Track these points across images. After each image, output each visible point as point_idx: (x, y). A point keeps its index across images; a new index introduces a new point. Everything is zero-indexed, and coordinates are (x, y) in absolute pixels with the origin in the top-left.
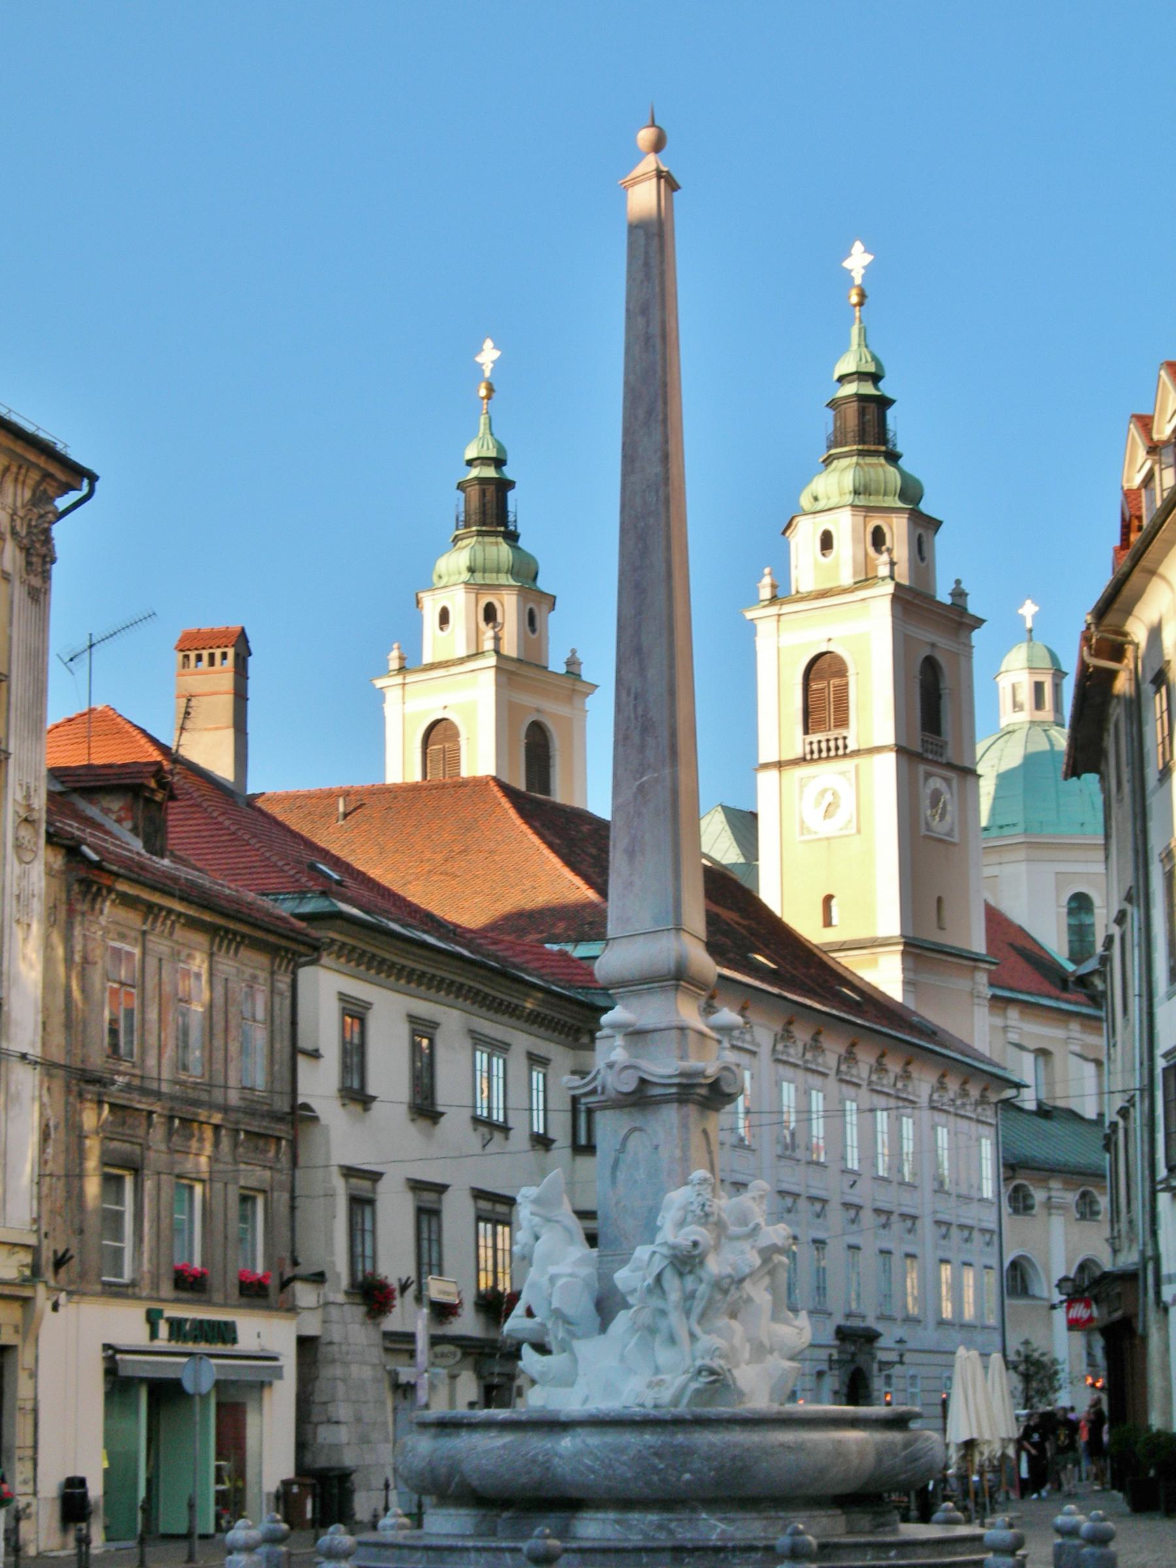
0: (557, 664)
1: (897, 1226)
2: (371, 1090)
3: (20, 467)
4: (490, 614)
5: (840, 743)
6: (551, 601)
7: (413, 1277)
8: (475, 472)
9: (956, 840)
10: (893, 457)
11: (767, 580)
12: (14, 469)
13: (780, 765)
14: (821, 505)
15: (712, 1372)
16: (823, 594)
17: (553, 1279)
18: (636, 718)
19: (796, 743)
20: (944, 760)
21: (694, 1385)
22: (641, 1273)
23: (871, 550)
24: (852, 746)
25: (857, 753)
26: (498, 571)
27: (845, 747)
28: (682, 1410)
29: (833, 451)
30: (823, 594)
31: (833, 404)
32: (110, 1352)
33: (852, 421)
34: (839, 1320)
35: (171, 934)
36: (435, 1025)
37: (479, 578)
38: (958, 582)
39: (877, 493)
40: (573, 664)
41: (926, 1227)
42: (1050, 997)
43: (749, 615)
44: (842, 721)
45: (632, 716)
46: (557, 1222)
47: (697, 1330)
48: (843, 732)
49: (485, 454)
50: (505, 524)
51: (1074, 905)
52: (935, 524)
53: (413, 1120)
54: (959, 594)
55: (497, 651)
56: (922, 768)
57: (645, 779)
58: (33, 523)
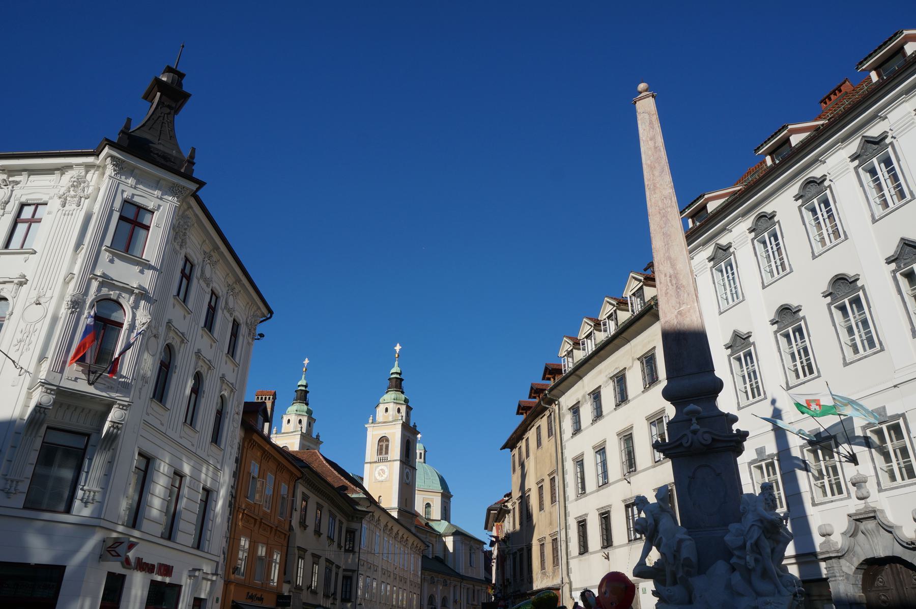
0: (314, 436)
2: (307, 524)
3: (252, 304)
4: (300, 422)
5: (386, 458)
6: (315, 420)
8: (300, 388)
10: (403, 393)
11: (371, 418)
12: (250, 304)
13: (370, 463)
14: (385, 402)
16: (384, 422)
18: (672, 285)
19: (375, 458)
22: (742, 537)
23: (397, 413)
26: (303, 412)
30: (384, 422)
31: (390, 379)
32: (235, 603)
33: (394, 384)
35: (268, 462)
36: (322, 507)
37: (298, 413)
38: (415, 423)
39: (399, 400)
40: (318, 436)
43: (366, 426)
44: (387, 453)
45: (669, 284)
46: (668, 512)
48: (386, 456)
49: (303, 384)
50: (306, 401)
52: (411, 409)
53: (315, 535)
54: (415, 426)
55: (301, 430)
57: (681, 309)
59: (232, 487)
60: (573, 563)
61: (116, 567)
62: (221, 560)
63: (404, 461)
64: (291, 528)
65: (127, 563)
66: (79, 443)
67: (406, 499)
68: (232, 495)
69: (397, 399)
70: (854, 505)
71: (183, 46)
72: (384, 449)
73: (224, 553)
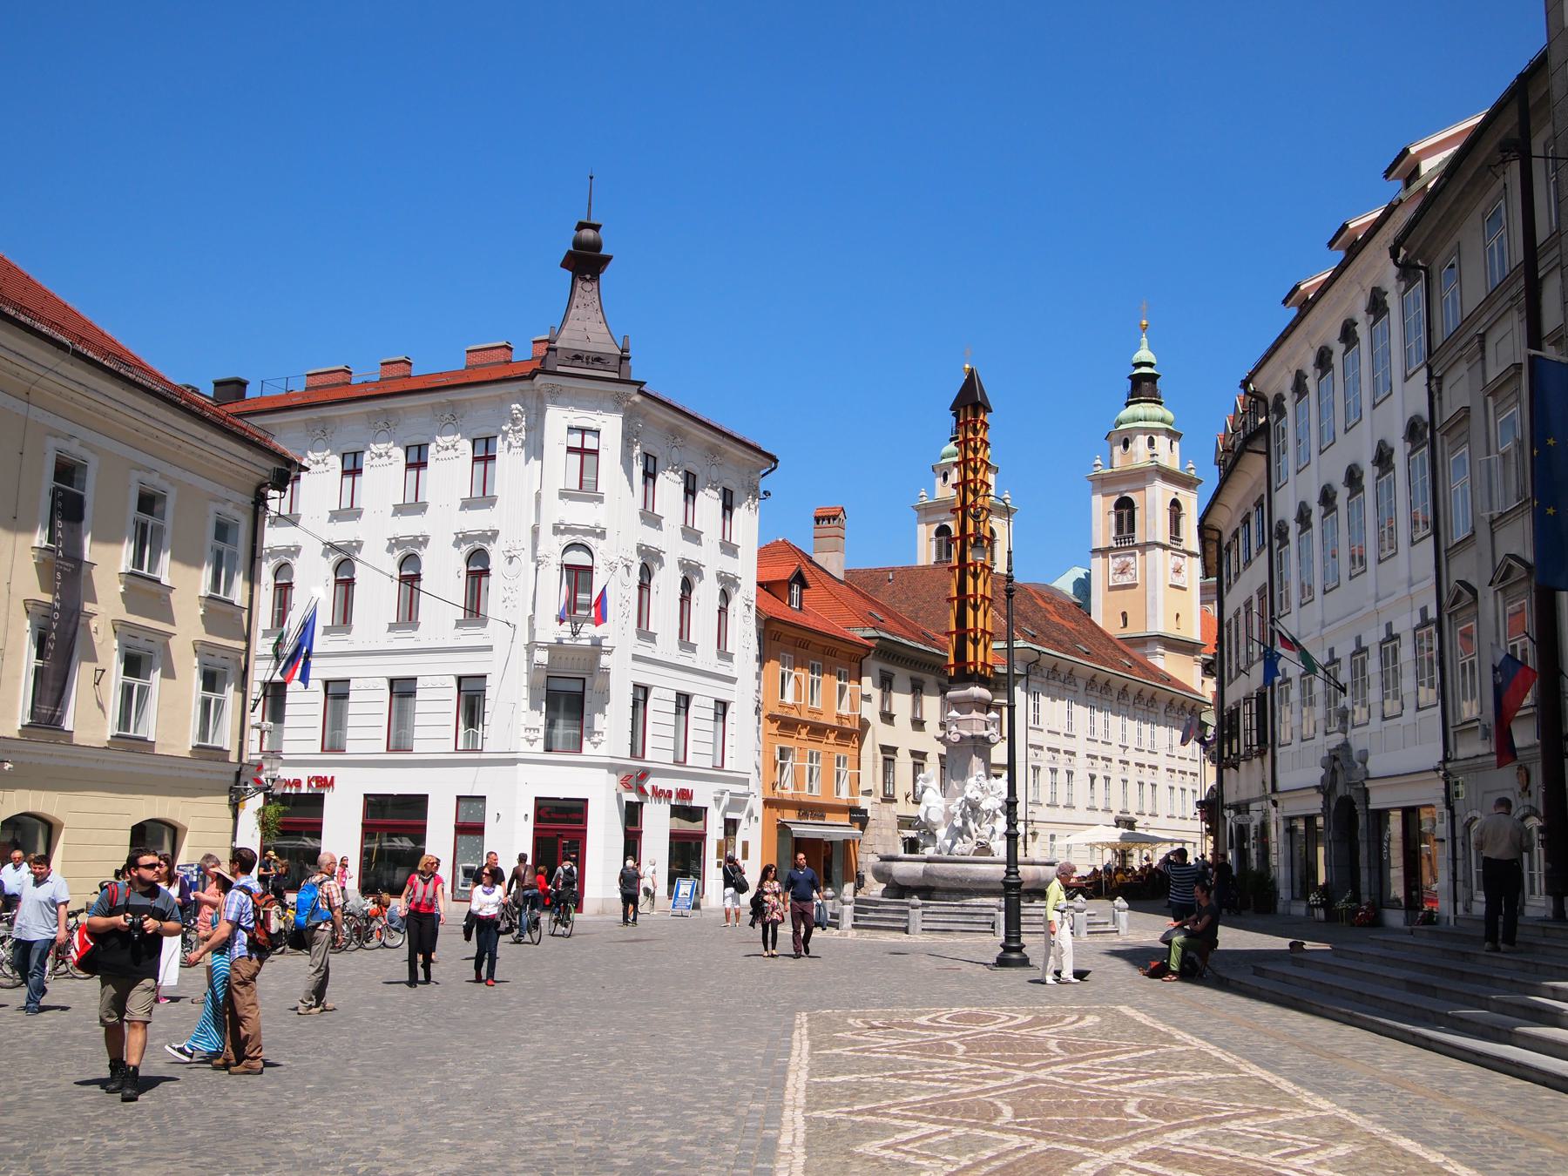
1: (1147, 771)
7: (912, 792)
15: (981, 844)
17: (928, 808)
20: (1181, 548)
21: (976, 848)
25: (1136, 546)
28: (971, 857)
34: (1116, 813)
39: (1150, 420)
41: (1162, 769)
44: (1132, 528)
47: (978, 828)
56: (1170, 551)
59: (757, 691)
60: (1225, 771)
61: (633, 797)
62: (753, 778)
63: (1167, 541)
64: (864, 725)
65: (642, 791)
66: (577, 687)
67: (1178, 616)
68: (759, 701)
69: (1145, 420)
70: (1336, 739)
71: (591, 178)
72: (1125, 522)
73: (757, 768)
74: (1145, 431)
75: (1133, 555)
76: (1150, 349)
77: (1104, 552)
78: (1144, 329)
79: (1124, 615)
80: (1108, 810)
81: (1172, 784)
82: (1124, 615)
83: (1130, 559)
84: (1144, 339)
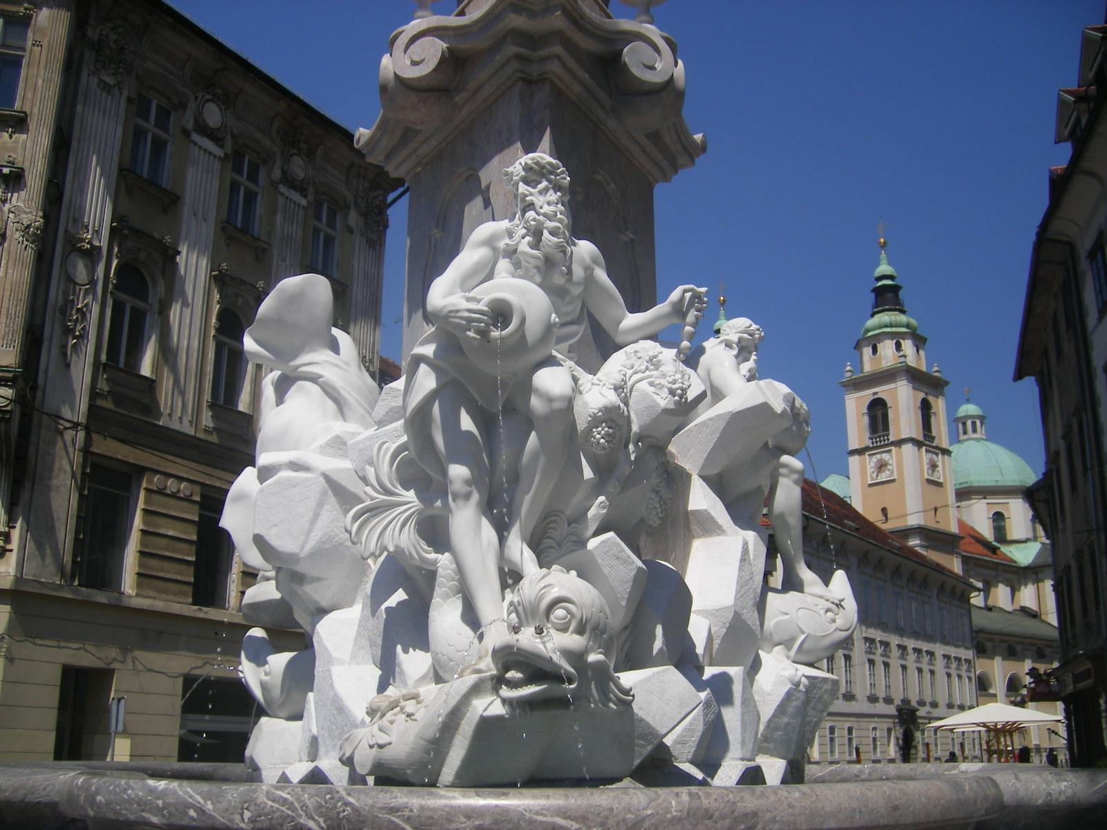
9: (941, 481)
15: (536, 669)
20: (934, 445)
24: (892, 439)
25: (893, 444)
27: (888, 440)
29: (875, 310)
42: (988, 557)
44: (886, 427)
46: (314, 379)
51: (995, 517)
58: (370, 201)
63: (921, 438)
69: (891, 326)
74: (891, 336)
75: (889, 451)
76: (889, 264)
77: (860, 452)
78: (884, 246)
79: (884, 510)
80: (888, 700)
81: (949, 671)
82: (884, 510)
83: (886, 457)
84: (883, 255)
